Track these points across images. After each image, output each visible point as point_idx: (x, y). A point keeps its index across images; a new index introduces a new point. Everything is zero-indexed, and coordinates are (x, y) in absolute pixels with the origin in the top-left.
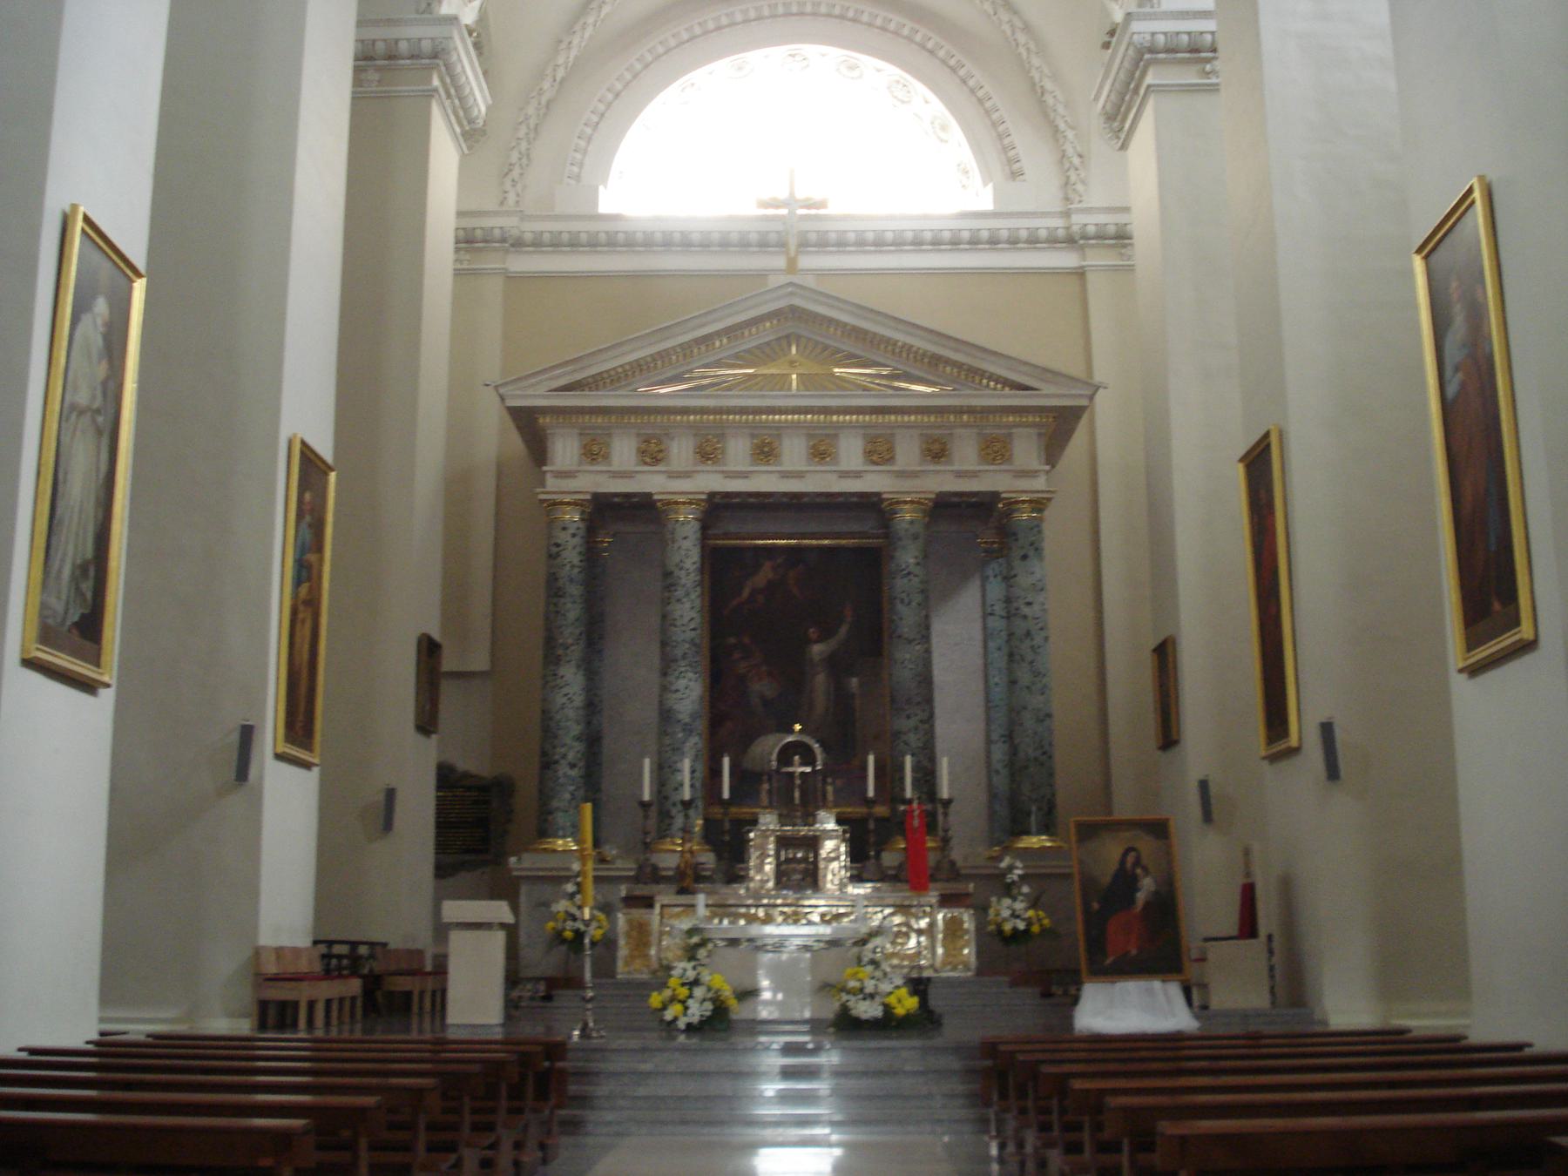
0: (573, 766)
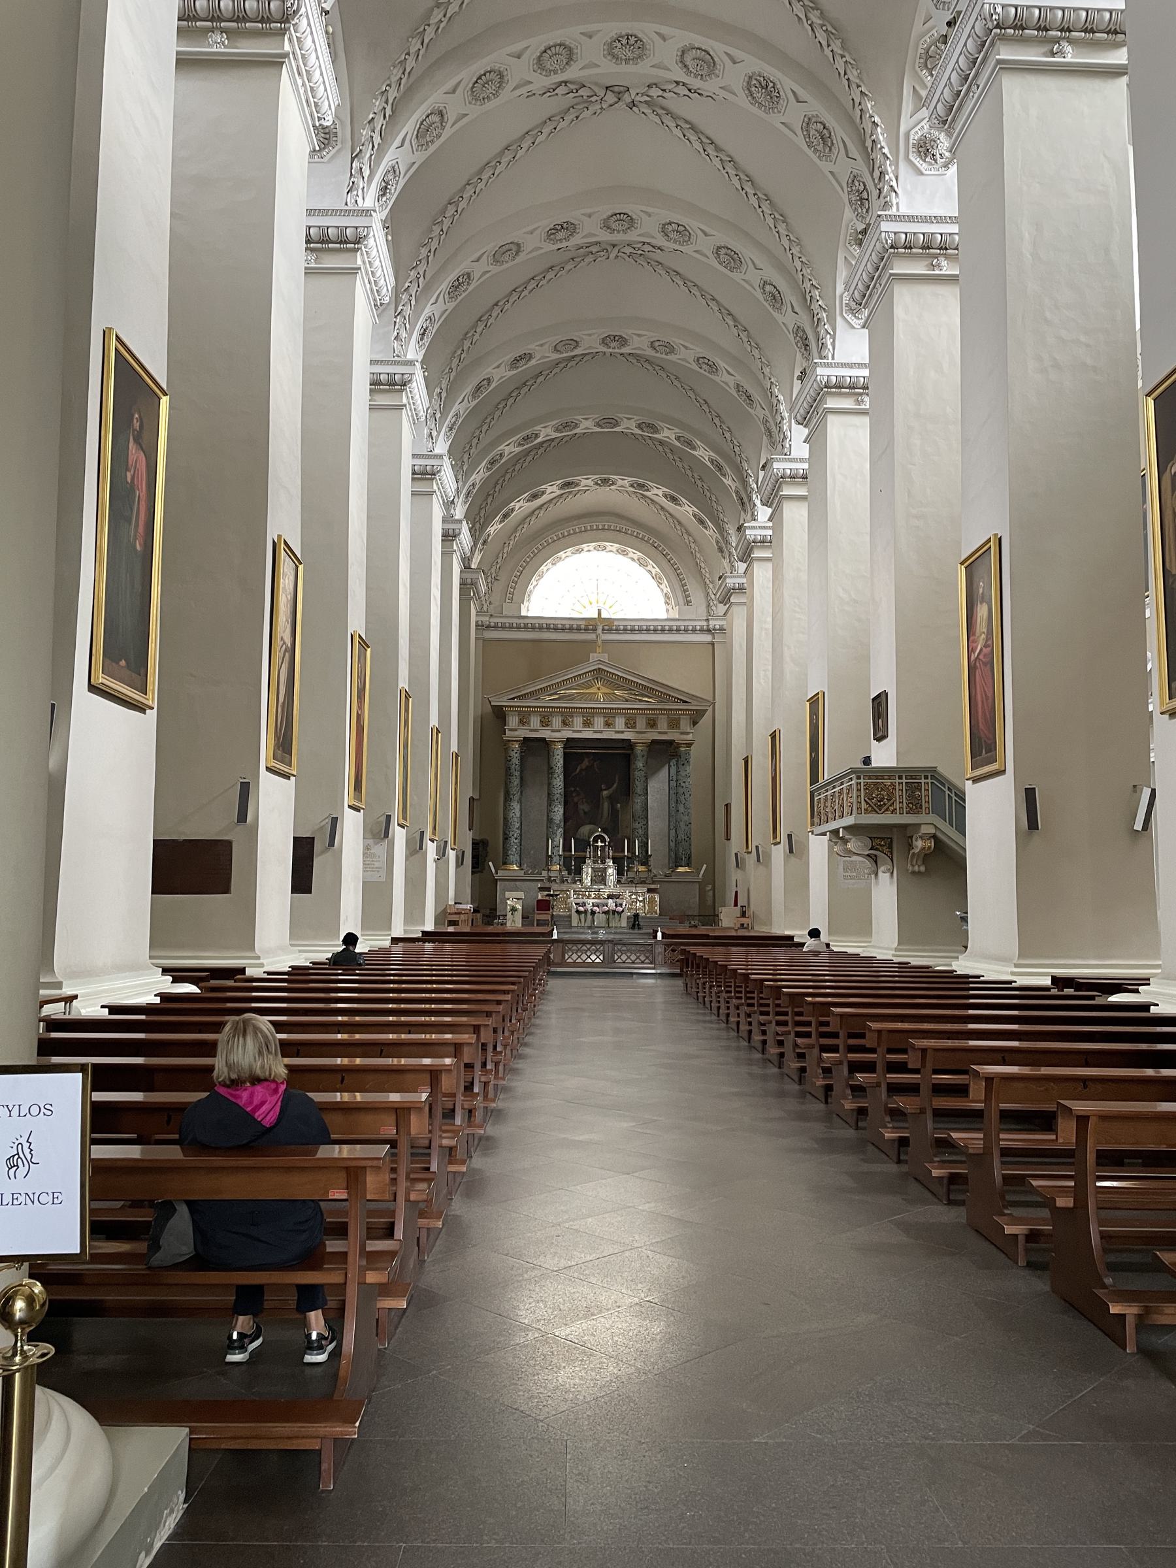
0: (516, 839)
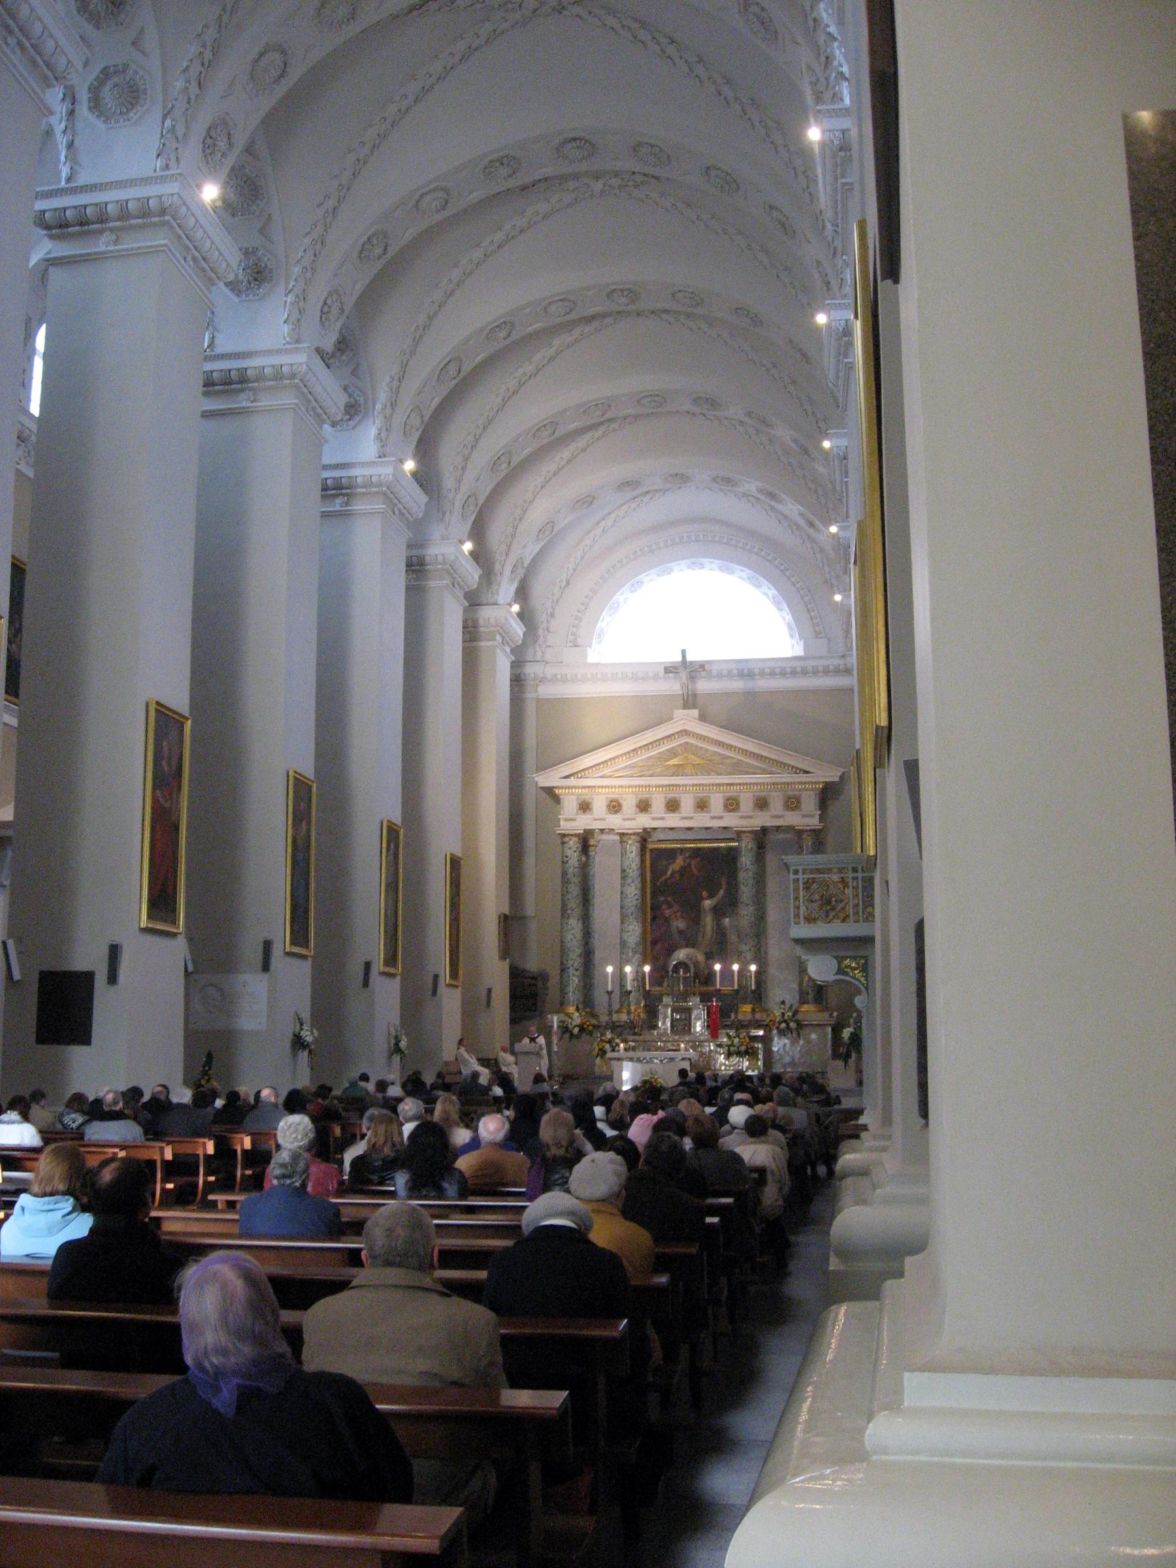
0: (577, 970)
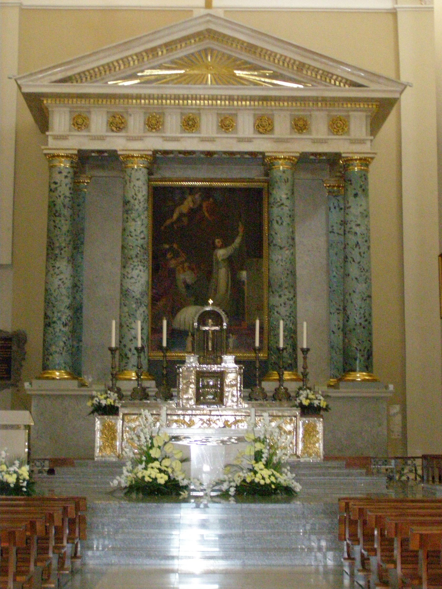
0: (65, 325)
